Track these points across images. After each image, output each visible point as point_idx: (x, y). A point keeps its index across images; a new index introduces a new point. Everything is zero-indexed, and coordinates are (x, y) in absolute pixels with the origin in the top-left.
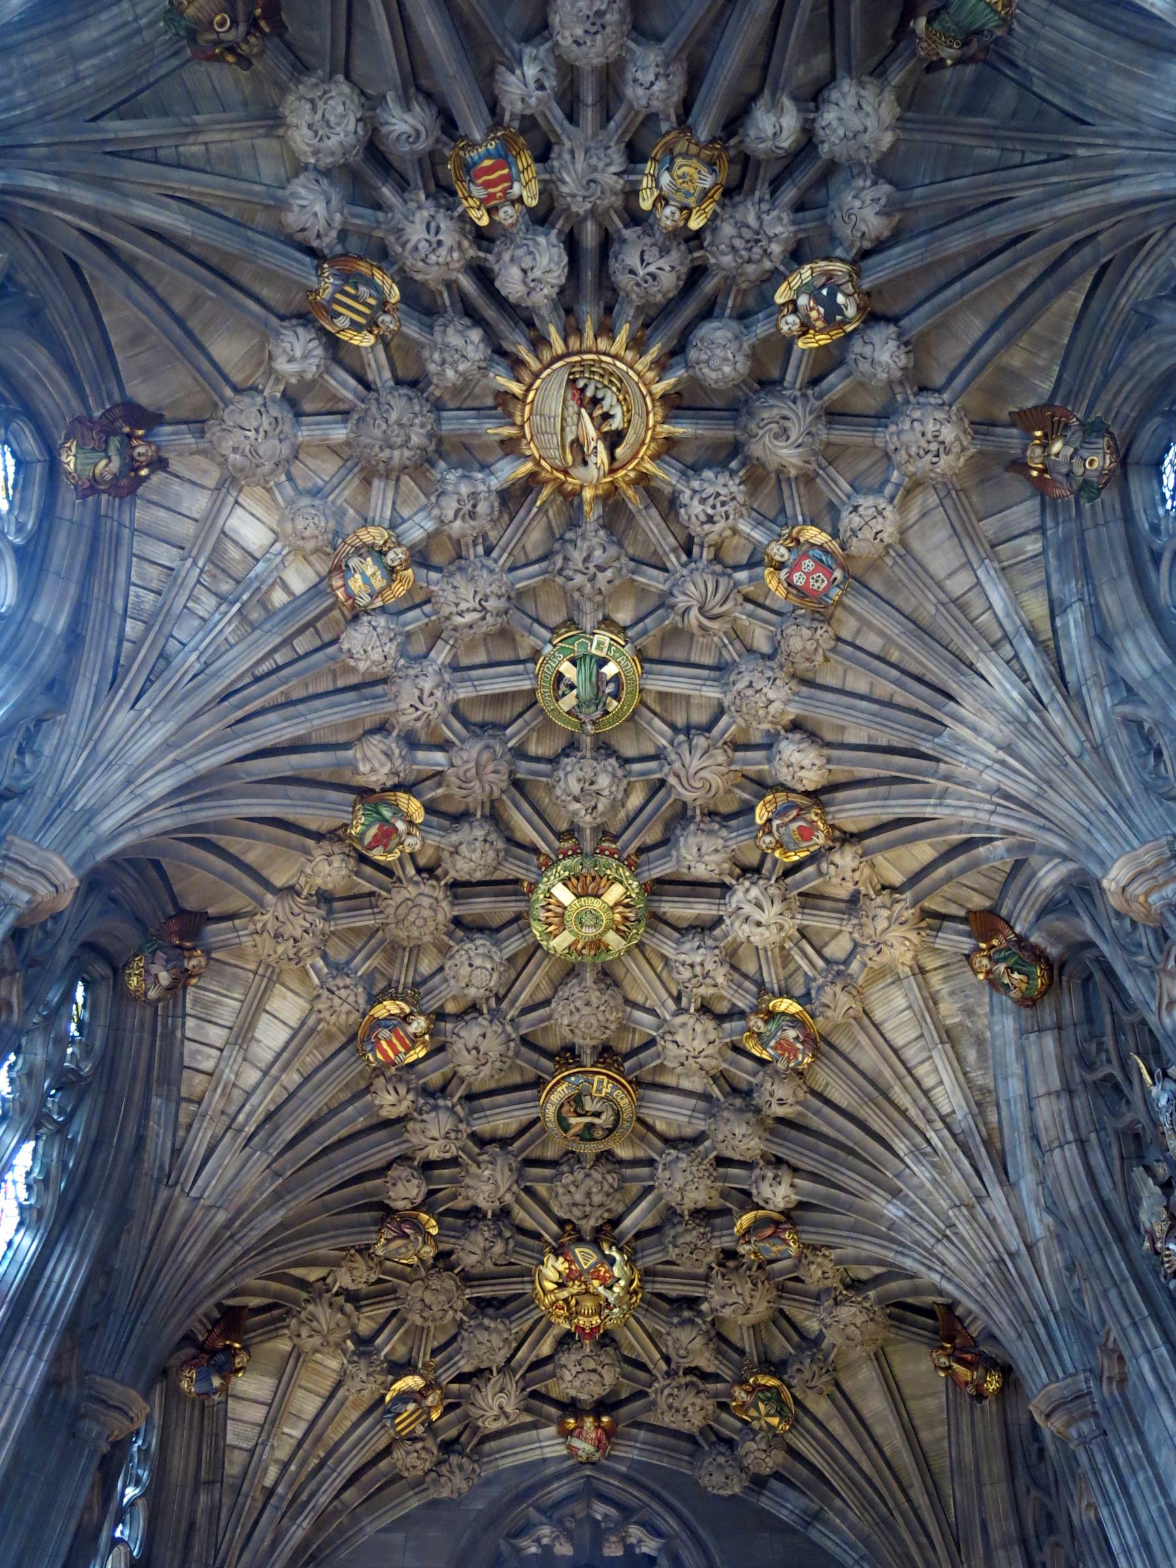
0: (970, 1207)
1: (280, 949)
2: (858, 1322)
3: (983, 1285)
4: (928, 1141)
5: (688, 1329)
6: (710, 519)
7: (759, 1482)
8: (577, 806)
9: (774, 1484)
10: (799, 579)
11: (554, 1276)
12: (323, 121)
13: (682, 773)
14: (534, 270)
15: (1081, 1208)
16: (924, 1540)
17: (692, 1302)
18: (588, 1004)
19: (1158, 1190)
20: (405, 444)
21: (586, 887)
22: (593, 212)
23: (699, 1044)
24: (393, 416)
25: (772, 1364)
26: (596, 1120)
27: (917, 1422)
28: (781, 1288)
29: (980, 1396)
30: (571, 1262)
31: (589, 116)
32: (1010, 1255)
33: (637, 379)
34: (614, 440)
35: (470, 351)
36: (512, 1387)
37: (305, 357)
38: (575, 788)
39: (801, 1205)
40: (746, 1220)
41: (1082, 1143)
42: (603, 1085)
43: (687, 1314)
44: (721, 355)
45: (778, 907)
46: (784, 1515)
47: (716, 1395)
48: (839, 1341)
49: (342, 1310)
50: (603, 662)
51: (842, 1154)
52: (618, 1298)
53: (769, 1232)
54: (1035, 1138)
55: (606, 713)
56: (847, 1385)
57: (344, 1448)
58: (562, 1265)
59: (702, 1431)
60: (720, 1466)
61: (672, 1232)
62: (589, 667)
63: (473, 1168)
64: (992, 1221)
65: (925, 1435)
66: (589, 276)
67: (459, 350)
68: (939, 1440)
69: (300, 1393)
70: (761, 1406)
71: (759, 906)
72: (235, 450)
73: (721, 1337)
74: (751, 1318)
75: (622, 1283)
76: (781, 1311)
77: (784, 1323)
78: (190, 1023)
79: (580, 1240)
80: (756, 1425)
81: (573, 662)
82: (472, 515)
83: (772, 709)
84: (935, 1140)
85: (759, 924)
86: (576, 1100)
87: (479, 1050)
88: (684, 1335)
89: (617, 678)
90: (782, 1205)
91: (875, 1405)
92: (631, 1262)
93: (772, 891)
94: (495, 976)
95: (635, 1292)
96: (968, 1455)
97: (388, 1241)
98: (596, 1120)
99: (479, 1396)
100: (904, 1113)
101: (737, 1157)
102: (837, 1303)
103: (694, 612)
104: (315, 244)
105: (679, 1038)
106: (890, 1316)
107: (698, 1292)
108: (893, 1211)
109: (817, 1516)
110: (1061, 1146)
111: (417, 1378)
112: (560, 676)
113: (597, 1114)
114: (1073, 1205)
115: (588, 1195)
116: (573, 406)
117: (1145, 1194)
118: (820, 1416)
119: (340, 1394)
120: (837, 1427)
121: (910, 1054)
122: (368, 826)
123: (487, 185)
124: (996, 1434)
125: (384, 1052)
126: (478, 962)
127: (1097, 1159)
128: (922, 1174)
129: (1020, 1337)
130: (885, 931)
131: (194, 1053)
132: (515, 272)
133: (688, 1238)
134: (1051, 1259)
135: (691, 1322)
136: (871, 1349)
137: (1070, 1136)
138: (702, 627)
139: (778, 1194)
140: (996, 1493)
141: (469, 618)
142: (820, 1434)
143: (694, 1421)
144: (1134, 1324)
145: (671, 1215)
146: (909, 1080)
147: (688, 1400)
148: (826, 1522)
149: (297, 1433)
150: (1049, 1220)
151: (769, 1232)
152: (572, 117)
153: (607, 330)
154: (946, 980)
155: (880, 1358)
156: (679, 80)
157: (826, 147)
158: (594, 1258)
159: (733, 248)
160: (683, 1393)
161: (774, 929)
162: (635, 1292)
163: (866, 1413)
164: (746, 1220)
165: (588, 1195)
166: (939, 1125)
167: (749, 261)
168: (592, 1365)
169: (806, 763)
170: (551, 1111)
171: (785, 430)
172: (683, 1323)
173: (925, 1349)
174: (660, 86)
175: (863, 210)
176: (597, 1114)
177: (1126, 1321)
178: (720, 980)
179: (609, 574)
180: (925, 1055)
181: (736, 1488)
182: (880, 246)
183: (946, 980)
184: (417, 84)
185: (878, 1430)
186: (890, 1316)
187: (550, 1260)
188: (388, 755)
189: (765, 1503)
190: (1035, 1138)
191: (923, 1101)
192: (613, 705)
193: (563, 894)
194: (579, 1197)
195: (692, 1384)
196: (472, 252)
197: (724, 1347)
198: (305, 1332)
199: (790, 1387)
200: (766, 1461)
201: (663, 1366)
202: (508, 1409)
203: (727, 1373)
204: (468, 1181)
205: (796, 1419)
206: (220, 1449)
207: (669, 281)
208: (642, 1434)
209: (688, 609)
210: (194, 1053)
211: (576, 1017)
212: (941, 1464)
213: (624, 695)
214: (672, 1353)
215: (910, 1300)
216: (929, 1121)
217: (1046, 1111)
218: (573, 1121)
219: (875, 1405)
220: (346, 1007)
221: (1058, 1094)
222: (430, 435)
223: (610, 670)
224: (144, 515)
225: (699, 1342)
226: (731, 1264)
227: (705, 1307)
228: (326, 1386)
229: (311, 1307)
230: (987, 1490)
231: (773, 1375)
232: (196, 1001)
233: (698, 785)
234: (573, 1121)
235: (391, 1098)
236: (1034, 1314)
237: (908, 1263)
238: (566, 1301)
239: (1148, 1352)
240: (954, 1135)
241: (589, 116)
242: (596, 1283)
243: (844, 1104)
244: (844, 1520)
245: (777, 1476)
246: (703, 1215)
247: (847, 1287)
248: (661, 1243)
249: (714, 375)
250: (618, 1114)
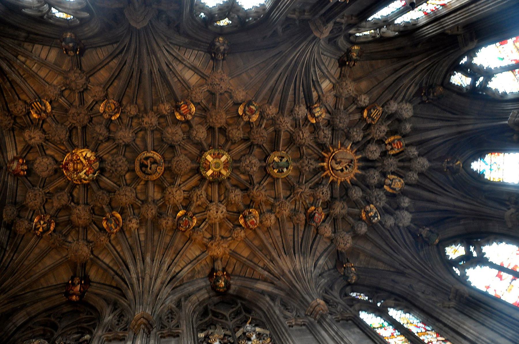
1: (217, 80)
5: (68, 199)
6: (323, 193)
8: (248, 162)
10: (317, 215)
11: (88, 155)
12: (407, 110)
13: (259, 189)
14: (374, 152)
18: (187, 165)
20: (340, 122)
21: (226, 165)
22: (384, 165)
23: (177, 198)
24: (346, 120)
26: (149, 168)
30: (94, 161)
31: (401, 164)
33: (350, 175)
34: (342, 170)
35: (359, 138)
36: (41, 141)
37: (365, 102)
38: (253, 161)
42: (161, 170)
43: (71, 198)
44: (356, 194)
45: (222, 217)
49: (82, 87)
50: (287, 168)
52: (81, 176)
53: (118, 223)
55: (274, 169)
57: (26, 84)
58: (93, 158)
60: (13, 213)
61: (105, 193)
62: (286, 164)
63: (131, 131)
65: (42, 280)
66: (370, 164)
67: (358, 135)
69: (48, 71)
71: (222, 212)
72: (346, 84)
75: (87, 178)
78: (196, 52)
79: (100, 163)
81: (287, 161)
82: (325, 137)
83: (284, 211)
85: (217, 212)
86: (155, 162)
87: (175, 134)
89: (283, 171)
91: (48, 262)
92: (93, 180)
93: (225, 215)
94: (199, 139)
95: (81, 181)
96: (44, 295)
97: (114, 104)
98: (149, 168)
99: (38, 130)
103: (301, 190)
104: (386, 107)
105: (178, 192)
111: (50, 110)
112: (283, 157)
113: (150, 169)
115: (120, 166)
116: (348, 161)
119: (46, 84)
120: (37, 251)
122: (256, 107)
123: (397, 144)
124: (57, 303)
125: (184, 107)
126: (203, 134)
130: (222, 246)
131: (189, 52)
132: (375, 149)
133: (106, 198)
138: (298, 193)
140: (40, 307)
141: (301, 135)
147: (39, 201)
149: (34, 68)
152: (399, 161)
153: (359, 168)
154: (205, 265)
156: (414, 183)
157: (399, 213)
158: (96, 168)
159: (378, 195)
161: (216, 217)
162: (81, 181)
165: (120, 166)
167: (376, 199)
168: (50, 168)
169: (272, 221)
170: (149, 155)
171: (342, 209)
172: (68, 197)
174: (414, 179)
175: (390, 222)
176: (150, 169)
178: (198, 203)
179: (307, 169)
181: (5, 219)
182: (383, 226)
183: (205, 265)
184: (415, 130)
187: (93, 154)
188: (273, 114)
192: (276, 171)
193: (224, 158)
194: (120, 163)
196: (376, 139)
198: (76, 75)
202: (33, 140)
204: (128, 130)
206: (33, 42)
207: (372, 181)
208: (15, 185)
209: (302, 189)
210: (189, 52)
211: (183, 162)
213: (278, 173)
218: (149, 161)
219: (48, 262)
220: (197, 97)
222: (340, 128)
223: (285, 170)
224: (333, 60)
225: (63, 202)
228: (49, 80)
229: (85, 77)
232: (201, 54)
233: (258, 194)
234: (149, 161)
235: (167, 108)
238: (79, 159)
241: (401, 164)
242: (87, 169)
249: (353, 192)
250: (150, 174)
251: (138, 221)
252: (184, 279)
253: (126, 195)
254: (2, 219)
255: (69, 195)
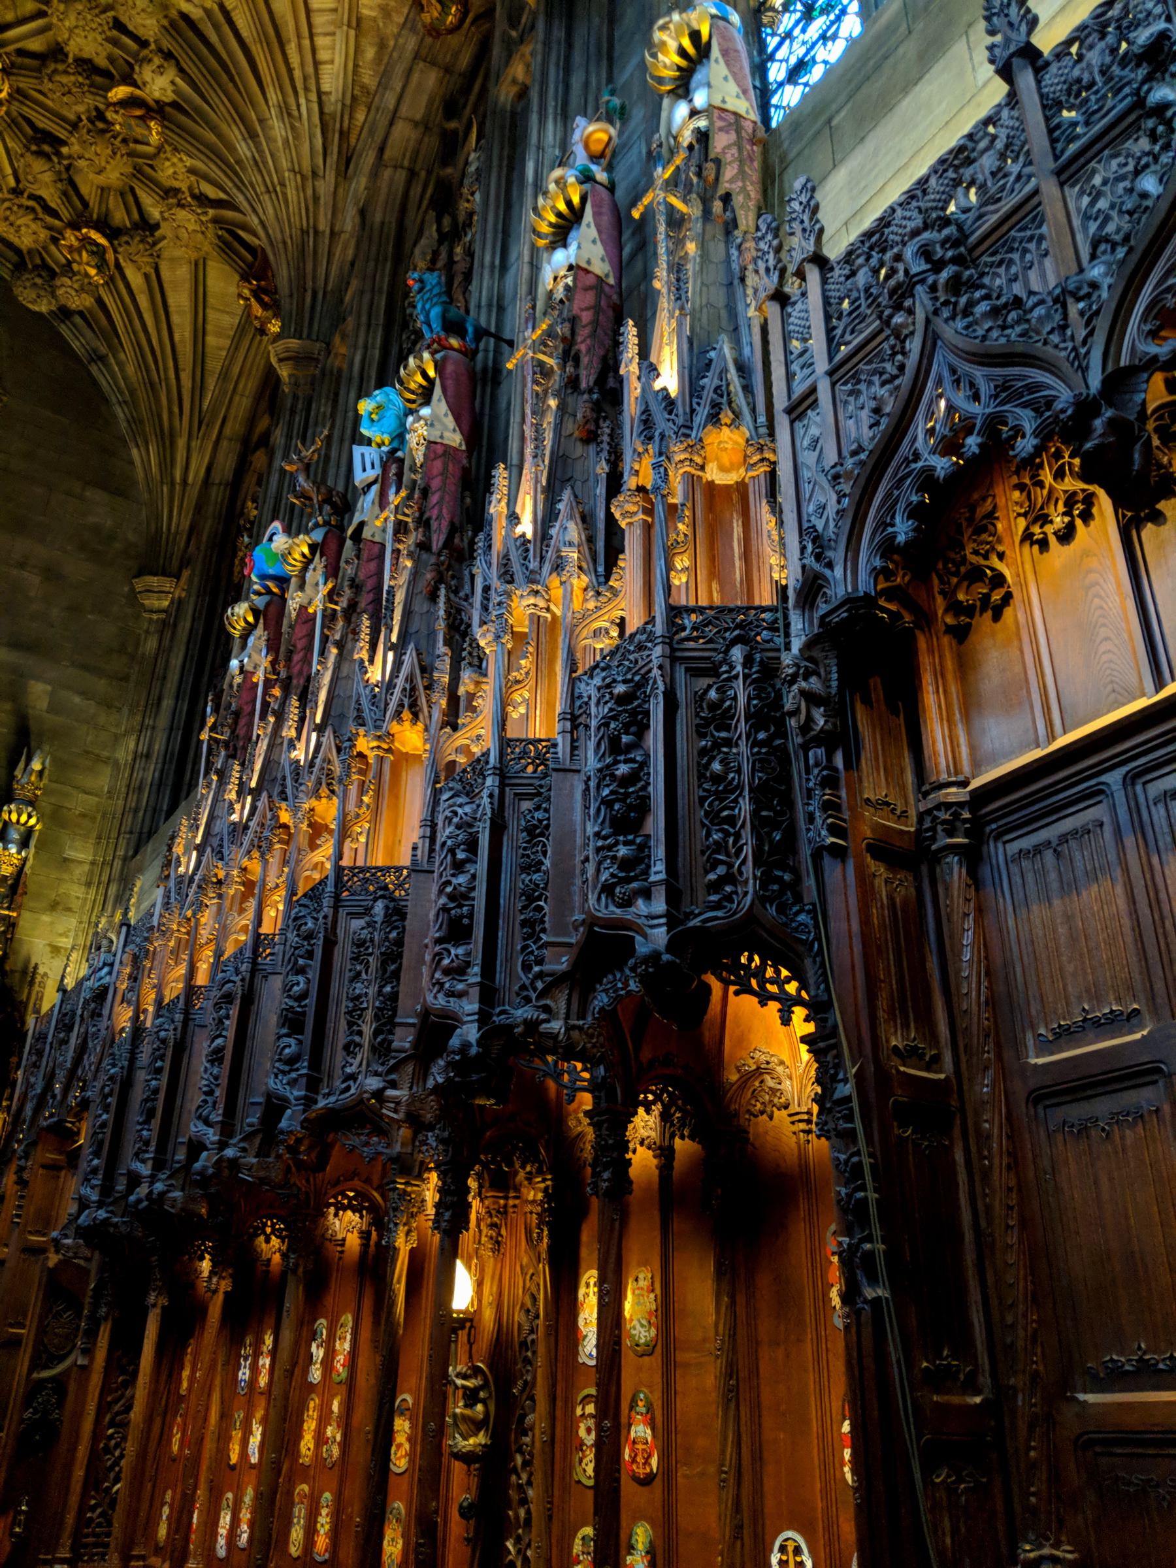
0: (303, 177)
2: (191, 227)
3: (285, 243)
4: (298, 106)
7: (65, 313)
9: (78, 319)
15: (383, 223)
16: (176, 410)
17: (58, 142)
19: (435, 235)
25: (110, 227)
27: (209, 327)
28: (138, 169)
29: (262, 331)
32: (316, 232)
39: (174, 105)
40: (120, 92)
41: (412, 173)
43: (47, 148)
46: (75, 345)
47: (50, 228)
48: (170, 235)
51: (225, 77)
53: (138, 113)
54: (382, 150)
56: (165, 274)
59: (30, 251)
60: (35, 284)
61: (52, 66)
64: (316, 199)
65: (211, 340)
68: (221, 349)
70: (84, 254)
73: (72, 183)
74: (101, 180)
76: (132, 189)
77: (130, 199)
80: (75, 267)
84: (304, 109)
88: (38, 165)
90: (157, 95)
96: (236, 370)
100: (290, 71)
101: (131, 28)
102: (180, 205)
106: (219, 237)
107: (62, 135)
108: (243, 149)
109: (102, 359)
110: (395, 167)
114: (378, 218)
117: (426, 233)
118: (133, 286)
120: (143, 301)
121: (319, 20)
127: (416, 190)
128: (278, 129)
129: (291, 296)
134: (345, 250)
135: (47, 157)
136: (194, 255)
137: (406, 163)
139: (159, 84)
142: (127, 300)
143: (25, 241)
144: (369, 325)
145: (57, 52)
146: (306, 43)
148: (107, 366)
150: (357, 220)
151: (138, 113)
155: (199, 268)
160: (21, 212)
163: (171, 301)
164: (120, 92)
166: (314, 97)
172: (40, 154)
173: (237, 277)
177: (364, 319)
180: (331, 29)
185: (175, 319)
186: (219, 237)
189: (64, 330)
190: (382, 150)
191: (310, 69)
195: (33, 210)
197: (71, 192)
199: (115, 251)
200: (79, 301)
201: (12, 182)
203: (65, 214)
205: (112, 278)
212: (214, 365)
214: (22, 177)
215: (241, 233)
216: (306, 89)
217: (403, 133)
219: (180, 300)
221: (416, 124)
226: (101, 125)
227: (65, 150)
230: (237, 398)
231: (105, 235)
236: (310, 284)
237: (240, 199)
239: (366, 348)
240: (321, 113)
243: (245, 33)
244: (122, 370)
245: (81, 314)
246: (86, 66)
247: (193, 196)
248: (39, 70)
251: (157, 61)
252: (366, 80)
253: (71, 30)
254: (40, 315)
255: (34, 148)
